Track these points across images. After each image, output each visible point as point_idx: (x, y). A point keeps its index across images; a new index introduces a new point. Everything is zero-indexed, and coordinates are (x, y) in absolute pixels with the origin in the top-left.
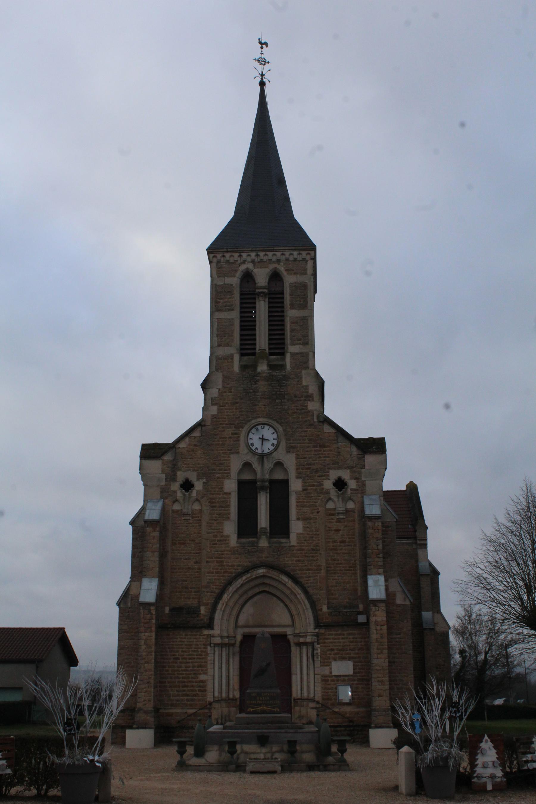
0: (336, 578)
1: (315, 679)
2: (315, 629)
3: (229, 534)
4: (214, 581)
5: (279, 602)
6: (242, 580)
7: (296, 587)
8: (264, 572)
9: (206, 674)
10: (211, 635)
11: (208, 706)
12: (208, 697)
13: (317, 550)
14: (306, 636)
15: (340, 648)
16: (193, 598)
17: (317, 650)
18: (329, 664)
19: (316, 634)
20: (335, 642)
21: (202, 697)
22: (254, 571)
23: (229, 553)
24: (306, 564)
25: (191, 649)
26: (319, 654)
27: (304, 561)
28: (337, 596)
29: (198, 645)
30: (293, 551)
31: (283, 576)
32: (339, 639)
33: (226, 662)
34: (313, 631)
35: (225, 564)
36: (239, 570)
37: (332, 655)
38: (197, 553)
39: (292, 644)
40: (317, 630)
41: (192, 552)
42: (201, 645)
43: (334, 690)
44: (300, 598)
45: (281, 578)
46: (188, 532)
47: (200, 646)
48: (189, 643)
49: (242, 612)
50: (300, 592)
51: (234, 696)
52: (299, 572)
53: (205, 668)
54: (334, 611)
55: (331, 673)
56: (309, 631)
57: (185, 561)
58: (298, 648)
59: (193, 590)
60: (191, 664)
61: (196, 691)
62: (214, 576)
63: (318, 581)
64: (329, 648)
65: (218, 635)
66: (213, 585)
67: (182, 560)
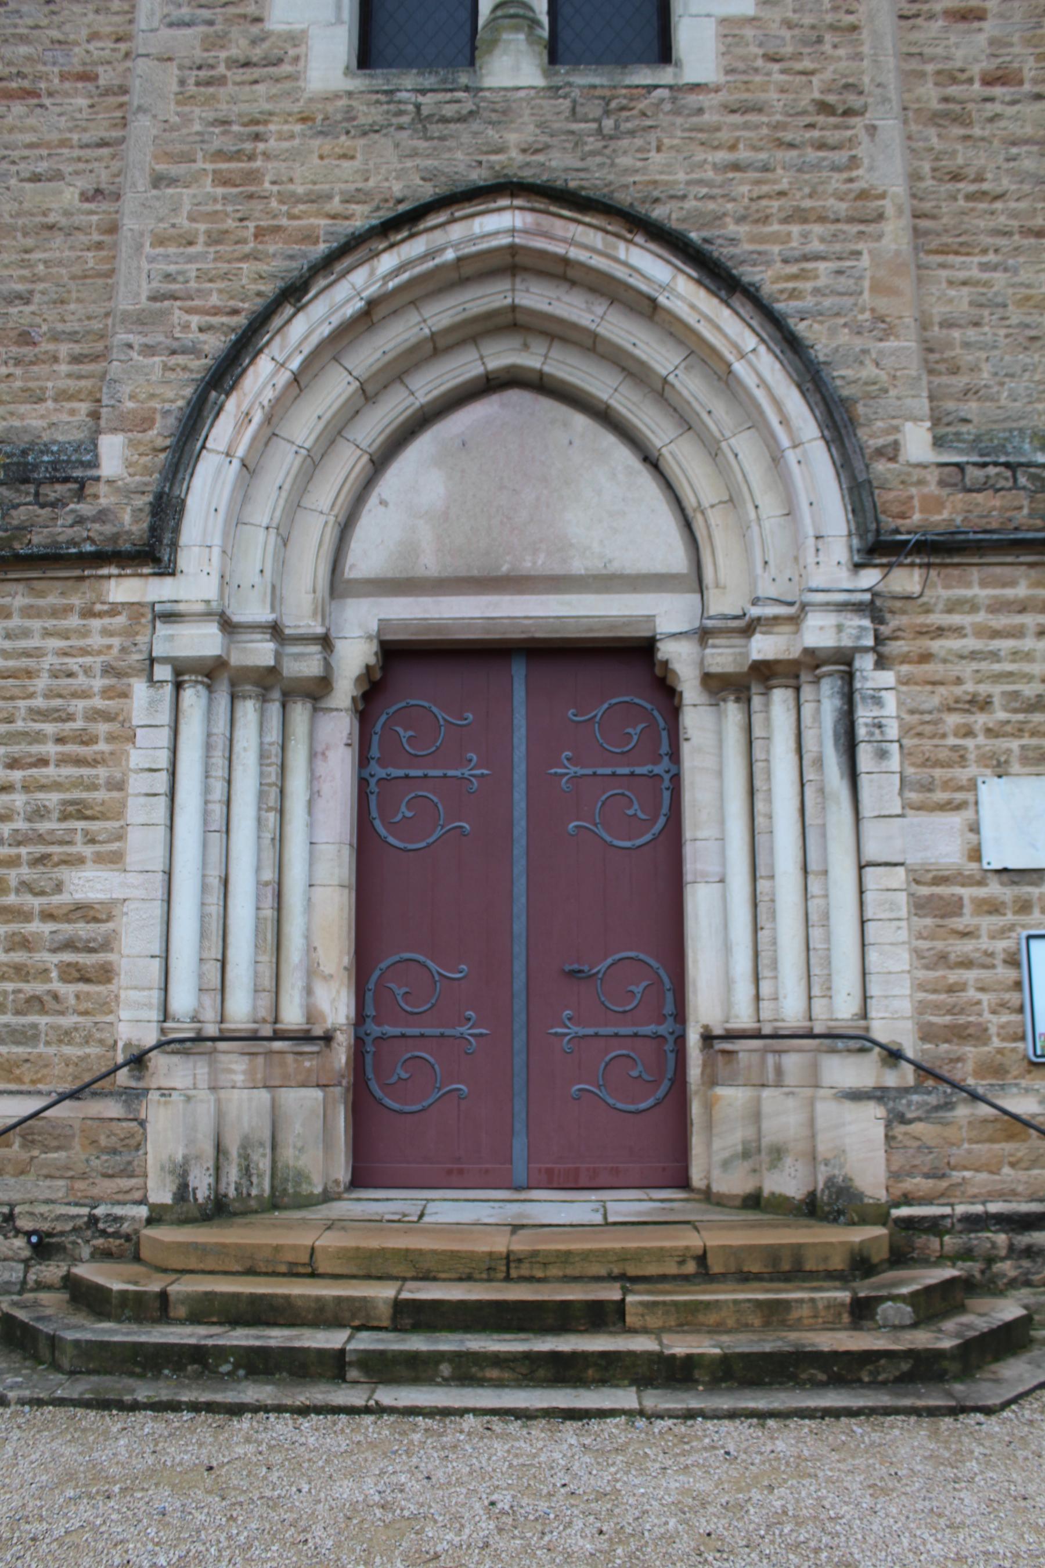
0: (975, 273)
1: (869, 897)
2: (858, 566)
3: (298, 27)
4: (193, 285)
5: (609, 440)
6: (372, 273)
7: (727, 312)
8: (513, 231)
9: (115, 859)
10: (157, 607)
11: (123, 1077)
12: (124, 1014)
13: (848, 113)
14: (795, 621)
16: (62, 396)
17: (878, 702)
18: (959, 796)
19: (867, 597)
20: (994, 656)
21: (86, 1013)
22: (453, 220)
23: (298, 128)
24: (784, 185)
25: (22, 704)
26: (893, 731)
27: (766, 169)
28: (985, 375)
29: (70, 675)
30: (700, 111)
31: (635, 251)
32: (1017, 633)
33: (262, 795)
34: (844, 578)
35: (267, 185)
36: (358, 224)
37: (981, 740)
38: (103, 144)
39: (690, 690)
40: (870, 577)
41: (75, 137)
42: (87, 671)
43: (1008, 974)
44: (750, 380)
45: (625, 264)
46: (55, 34)
47: (81, 680)
48: (11, 663)
49: (373, 501)
50: (750, 341)
51: (312, 1015)
52: (743, 229)
53: (116, 824)
55: (976, 854)
56: (817, 580)
57: (28, 186)
58: (733, 711)
59: (64, 349)
60: (18, 800)
61: (44, 974)
62: (191, 259)
63: (866, 284)
64: (958, 691)
65: (200, 607)
66: (189, 311)
67: (13, 182)
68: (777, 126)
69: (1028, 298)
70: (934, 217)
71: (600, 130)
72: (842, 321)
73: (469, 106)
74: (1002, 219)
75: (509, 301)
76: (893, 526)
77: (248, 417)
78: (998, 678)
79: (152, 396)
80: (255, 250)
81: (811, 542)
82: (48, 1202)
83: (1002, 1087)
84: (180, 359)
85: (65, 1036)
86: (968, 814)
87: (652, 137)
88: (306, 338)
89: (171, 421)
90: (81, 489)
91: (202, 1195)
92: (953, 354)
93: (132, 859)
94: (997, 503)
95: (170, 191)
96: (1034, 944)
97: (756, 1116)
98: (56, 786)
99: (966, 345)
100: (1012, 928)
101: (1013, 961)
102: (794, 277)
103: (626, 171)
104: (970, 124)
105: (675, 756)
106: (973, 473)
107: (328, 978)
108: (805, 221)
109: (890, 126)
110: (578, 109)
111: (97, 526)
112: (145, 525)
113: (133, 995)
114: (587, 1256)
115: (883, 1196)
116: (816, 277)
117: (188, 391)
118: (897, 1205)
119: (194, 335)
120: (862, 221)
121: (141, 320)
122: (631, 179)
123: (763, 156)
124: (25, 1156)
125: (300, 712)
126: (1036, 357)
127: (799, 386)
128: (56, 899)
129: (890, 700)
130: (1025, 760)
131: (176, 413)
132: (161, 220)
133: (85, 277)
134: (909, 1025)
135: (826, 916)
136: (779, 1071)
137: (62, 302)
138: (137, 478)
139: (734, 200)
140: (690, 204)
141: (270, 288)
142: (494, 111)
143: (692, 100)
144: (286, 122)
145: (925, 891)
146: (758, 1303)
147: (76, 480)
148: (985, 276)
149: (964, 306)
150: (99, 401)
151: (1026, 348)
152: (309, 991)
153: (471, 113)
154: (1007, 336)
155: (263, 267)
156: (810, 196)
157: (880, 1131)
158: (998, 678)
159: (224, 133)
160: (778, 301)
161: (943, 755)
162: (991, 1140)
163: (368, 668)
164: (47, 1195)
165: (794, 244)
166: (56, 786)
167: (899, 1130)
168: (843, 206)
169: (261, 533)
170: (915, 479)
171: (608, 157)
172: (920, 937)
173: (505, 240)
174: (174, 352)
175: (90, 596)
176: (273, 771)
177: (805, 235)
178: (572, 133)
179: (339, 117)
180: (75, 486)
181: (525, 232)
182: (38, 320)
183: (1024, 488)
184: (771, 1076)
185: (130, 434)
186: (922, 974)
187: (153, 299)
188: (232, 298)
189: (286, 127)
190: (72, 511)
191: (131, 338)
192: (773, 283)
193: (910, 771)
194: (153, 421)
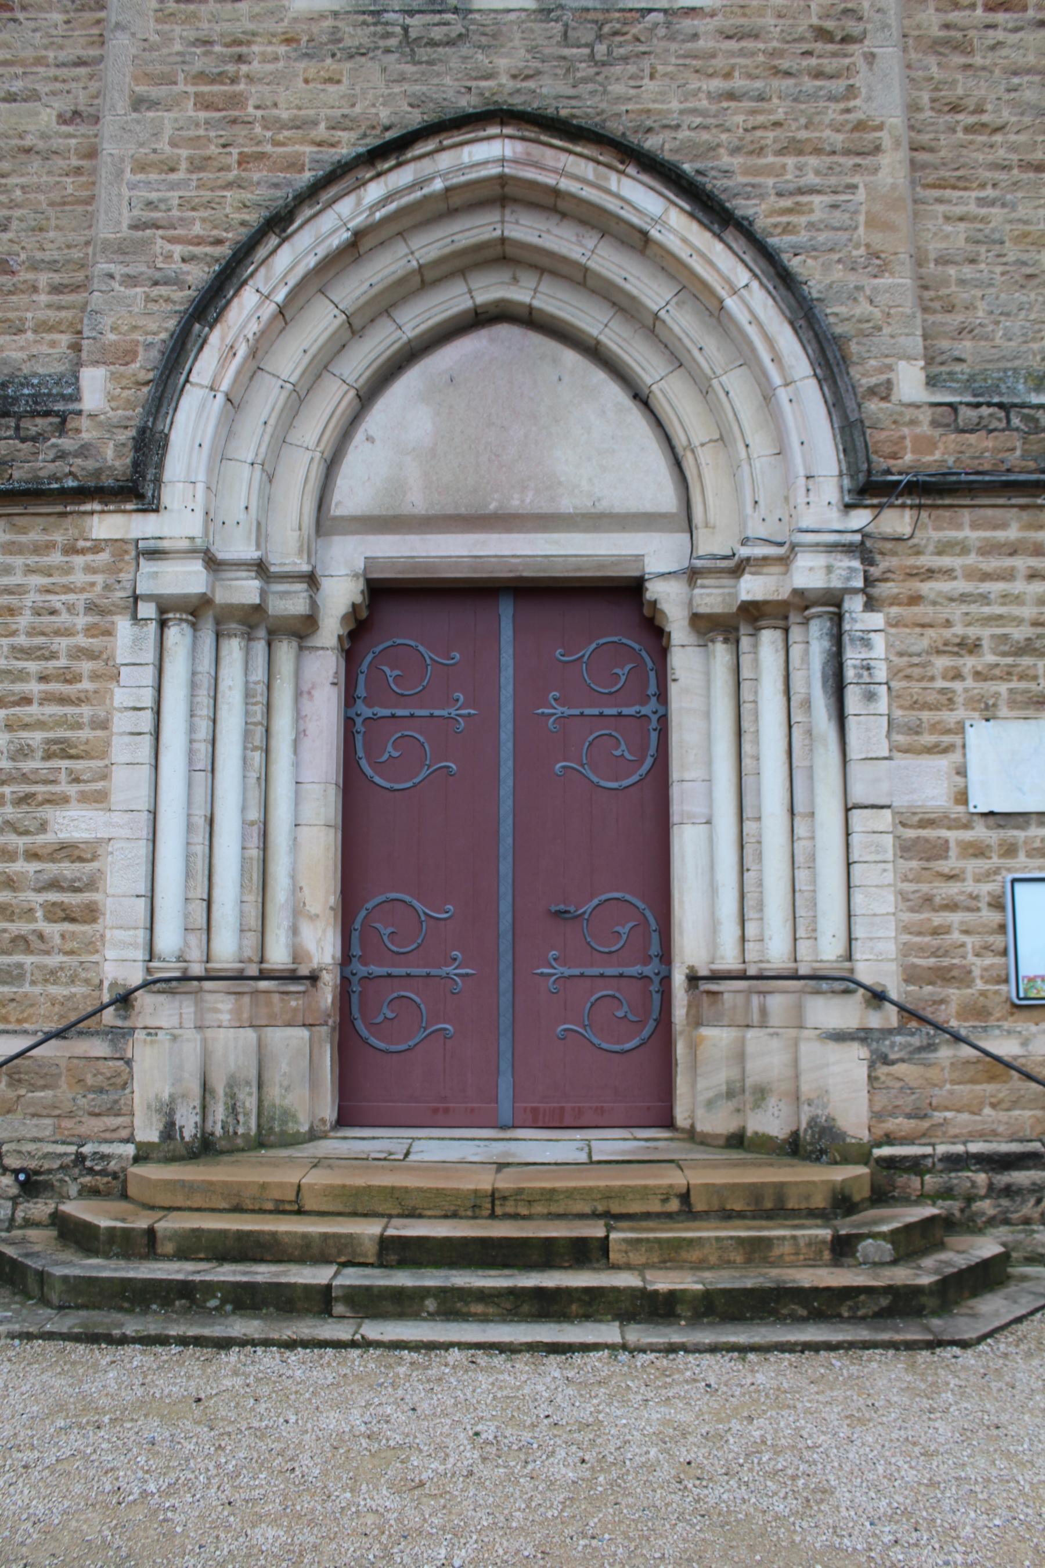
0: (973, 208)
1: (855, 839)
2: (848, 507)
4: (175, 213)
5: (599, 376)
7: (719, 246)
8: (503, 160)
9: (99, 799)
10: (141, 544)
11: (109, 1016)
12: (110, 954)
13: (846, 40)
14: (785, 561)
15: (1019, 634)
16: (42, 327)
17: (867, 644)
18: (947, 739)
19: (858, 537)
20: (984, 599)
21: (71, 953)
22: (442, 149)
23: (282, 49)
24: (780, 115)
26: (881, 673)
27: (761, 98)
28: (980, 314)
29: (53, 612)
30: (695, 36)
31: (625, 181)
32: (1008, 575)
33: (247, 735)
34: (834, 519)
35: (251, 110)
36: (344, 151)
37: (970, 683)
39: (678, 630)
40: (860, 518)
42: (70, 609)
43: (993, 917)
44: (742, 317)
47: (64, 618)
49: (359, 437)
50: (742, 276)
51: (297, 955)
53: (100, 763)
54: (969, 399)
55: (962, 797)
58: (721, 652)
59: (43, 279)
61: (29, 913)
62: (173, 186)
63: (862, 218)
64: (947, 633)
65: (184, 544)
66: (171, 240)
68: (773, 54)
69: (1025, 235)
70: (932, 150)
71: (592, 55)
72: (836, 257)
73: (458, 29)
74: (1002, 152)
75: (498, 233)
76: (884, 466)
77: (232, 350)
78: (988, 620)
79: (135, 328)
80: (238, 178)
81: (801, 481)
82: (34, 1140)
83: (985, 1029)
84: (163, 290)
85: (51, 975)
86: (956, 757)
87: (646, 63)
88: (292, 269)
89: (154, 354)
90: (62, 423)
91: (188, 1135)
92: (947, 291)
93: (117, 798)
94: (990, 444)
95: (151, 114)
96: (1018, 887)
97: (740, 1056)
98: (40, 725)
99: (962, 282)
100: (997, 871)
101: (998, 904)
102: (789, 211)
103: (619, 99)
104: (971, 53)
105: (663, 696)
106: (965, 413)
107: (314, 918)
108: (800, 153)
109: (889, 54)
110: (570, 33)
111: (79, 461)
112: (128, 461)
113: (120, 934)
114: (571, 1194)
115: (865, 1136)
116: (811, 211)
117: (172, 324)
118: (879, 1145)
119: (177, 265)
120: (859, 154)
121: (122, 250)
122: (624, 108)
123: (759, 84)
124: (11, 1094)
125: (286, 651)
126: (1033, 296)
127: (792, 323)
128: (40, 839)
129: (879, 641)
130: (1013, 704)
131: (159, 346)
132: (141, 145)
133: (64, 204)
134: (893, 967)
135: (812, 857)
136: (763, 1011)
137: (41, 230)
138: (120, 412)
139: (729, 130)
140: (684, 134)
141: (255, 218)
142: (484, 34)
143: (687, 24)
144: (270, 43)
145: (911, 833)
146: (740, 1240)
147: (57, 414)
148: (983, 211)
149: (961, 242)
150: (80, 332)
151: (1022, 286)
152: (295, 931)
153: (460, 35)
154: (1003, 274)
155: (246, 196)
156: (806, 127)
157: (863, 1071)
158: (988, 620)
159: (206, 54)
160: (772, 235)
161: (932, 697)
162: (973, 1081)
163: (354, 606)
164: (35, 1133)
165: (789, 177)
166: (40, 725)
167: (882, 1070)
168: (840, 137)
169: (246, 469)
170: (907, 419)
171: (601, 85)
172: (906, 879)
173: (494, 170)
174: (156, 283)
175: (73, 532)
176: (259, 710)
177: (800, 168)
178: (564, 58)
179: (324, 38)
180: (57, 420)
181: (515, 161)
182: (16, 248)
183: (1017, 429)
184: (756, 1017)
185: (112, 367)
186: (907, 917)
187: (134, 227)
188: (215, 227)
189: (269, 49)
190: (54, 446)
191: (112, 268)
192: (766, 217)
193: (898, 713)
194: (135, 354)
